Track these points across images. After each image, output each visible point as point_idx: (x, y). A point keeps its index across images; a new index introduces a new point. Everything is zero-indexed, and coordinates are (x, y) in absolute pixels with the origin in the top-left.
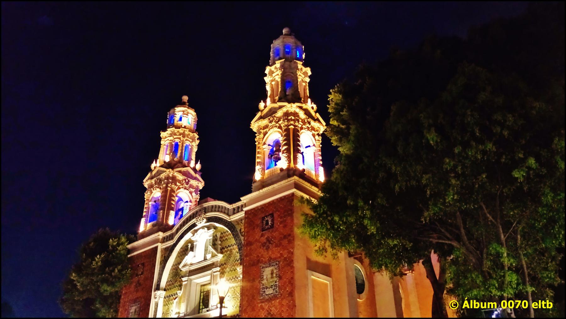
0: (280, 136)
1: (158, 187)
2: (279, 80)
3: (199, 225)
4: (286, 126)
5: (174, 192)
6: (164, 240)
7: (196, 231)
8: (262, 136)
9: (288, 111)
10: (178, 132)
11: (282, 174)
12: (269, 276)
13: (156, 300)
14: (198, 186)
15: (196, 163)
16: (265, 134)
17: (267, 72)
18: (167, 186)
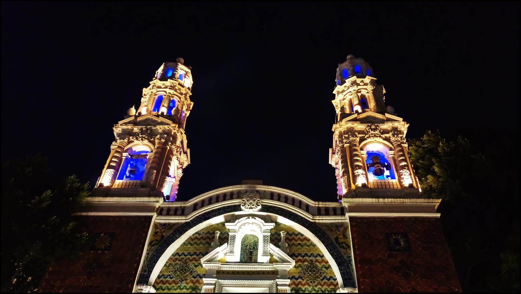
3: (245, 211)
8: (358, 139)
10: (180, 89)
16: (362, 140)
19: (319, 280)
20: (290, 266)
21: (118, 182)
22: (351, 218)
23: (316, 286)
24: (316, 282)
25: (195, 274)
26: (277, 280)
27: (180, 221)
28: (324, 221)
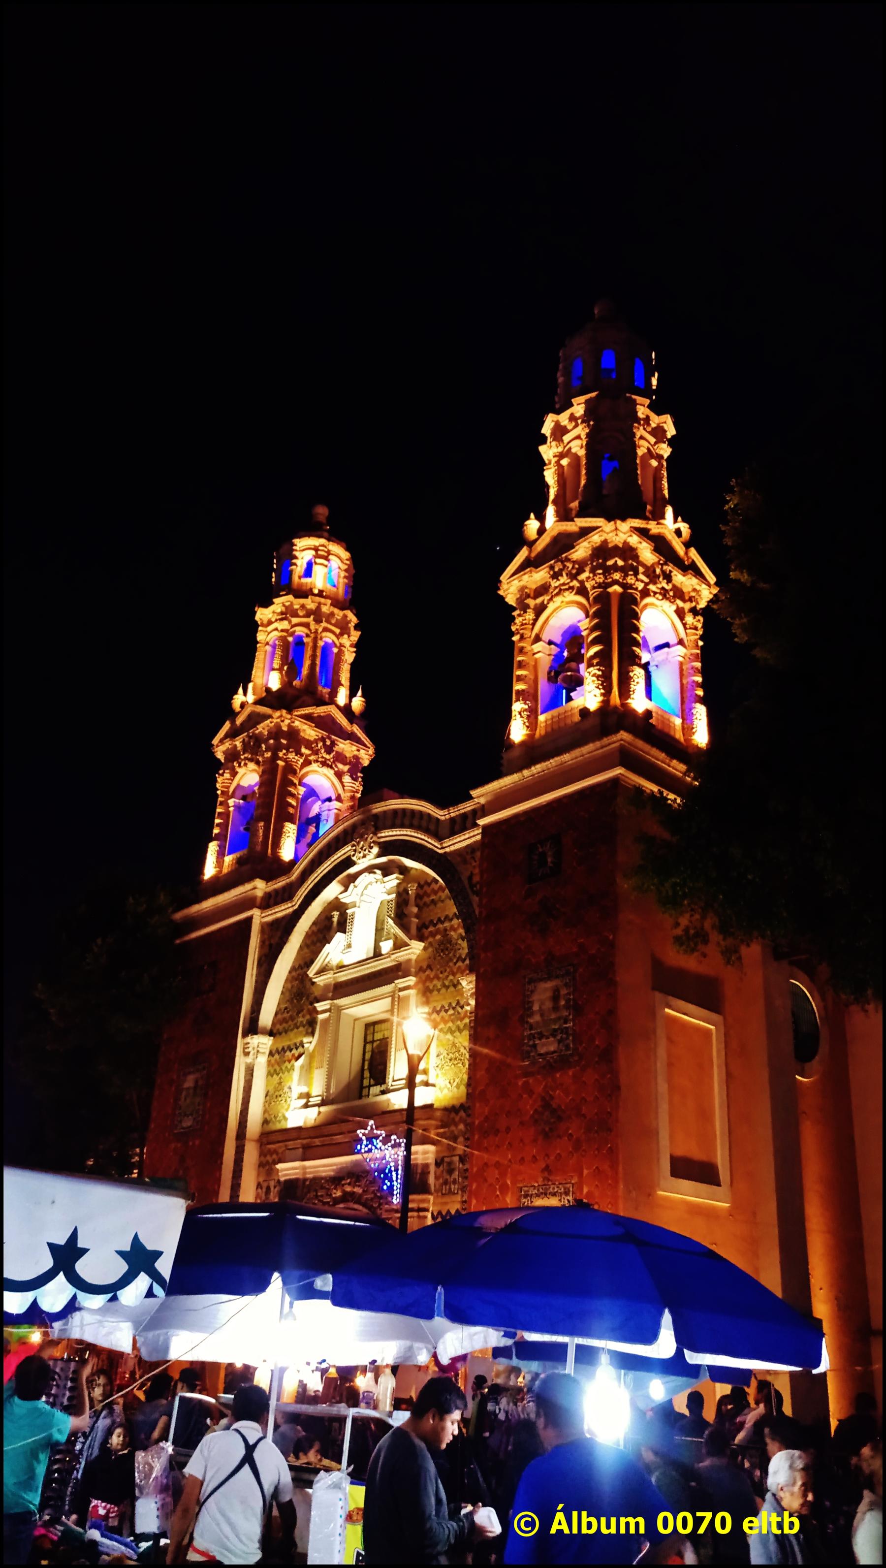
0: (581, 614)
1: (251, 760)
2: (582, 453)
4: (600, 585)
5: (294, 772)
6: (269, 901)
7: (353, 878)
8: (530, 616)
9: (605, 542)
10: (303, 606)
11: (589, 723)
12: (549, 1005)
13: (249, 1060)
14: (357, 758)
15: (352, 694)
16: (540, 610)
17: (547, 429)
18: (275, 757)
19: (451, 964)
20: (416, 949)
21: (228, 859)
22: (486, 828)
23: (447, 977)
24: (448, 970)
25: (311, 998)
26: (396, 982)
27: (287, 911)
28: (457, 846)
